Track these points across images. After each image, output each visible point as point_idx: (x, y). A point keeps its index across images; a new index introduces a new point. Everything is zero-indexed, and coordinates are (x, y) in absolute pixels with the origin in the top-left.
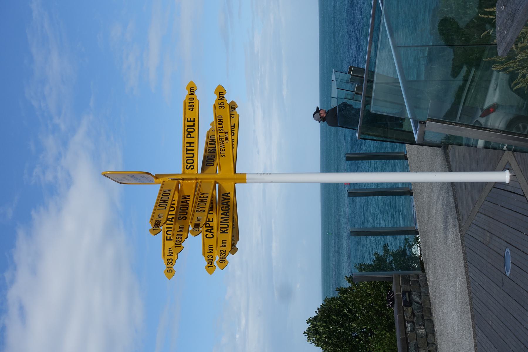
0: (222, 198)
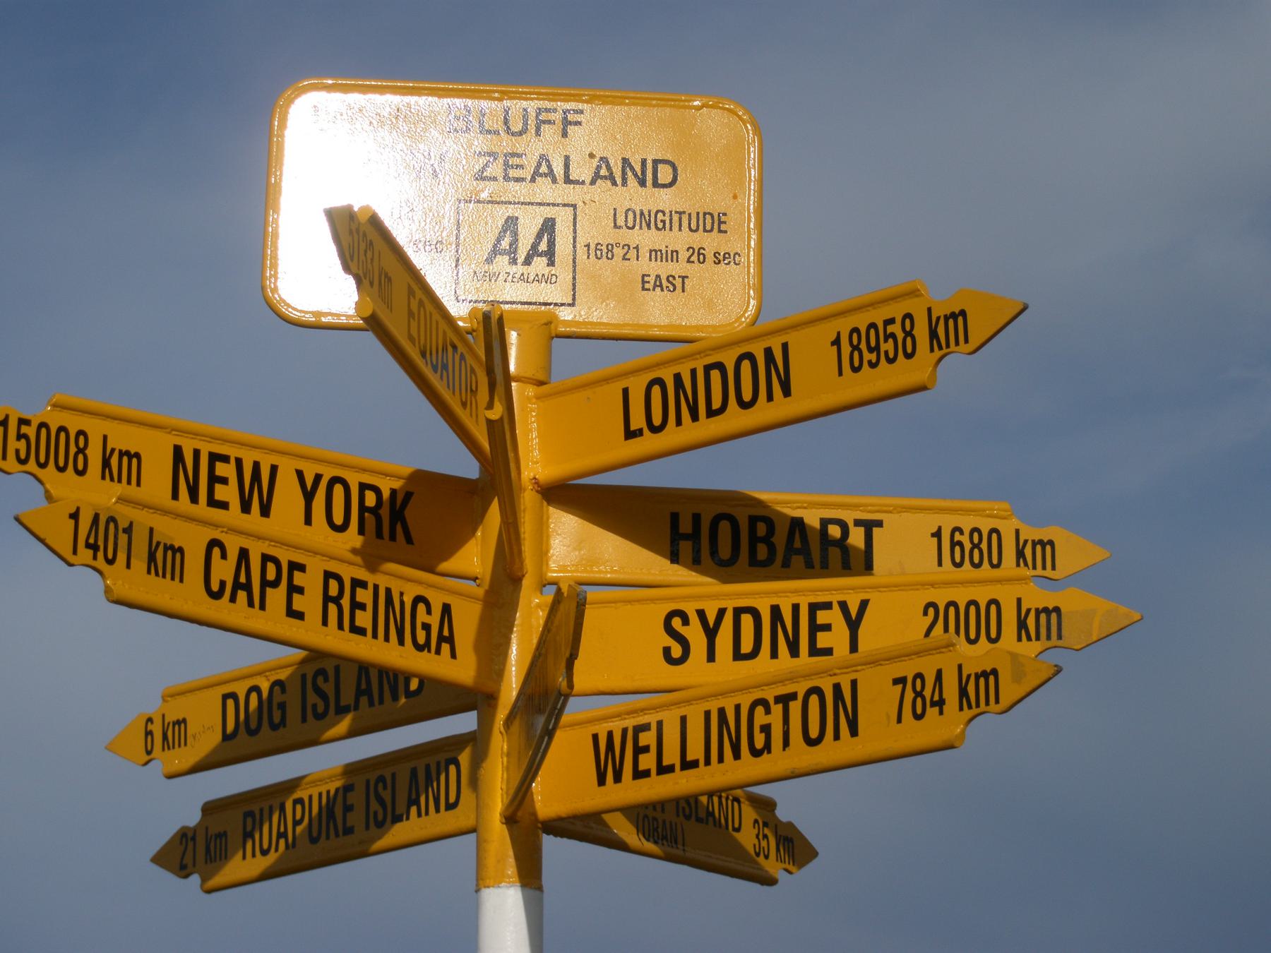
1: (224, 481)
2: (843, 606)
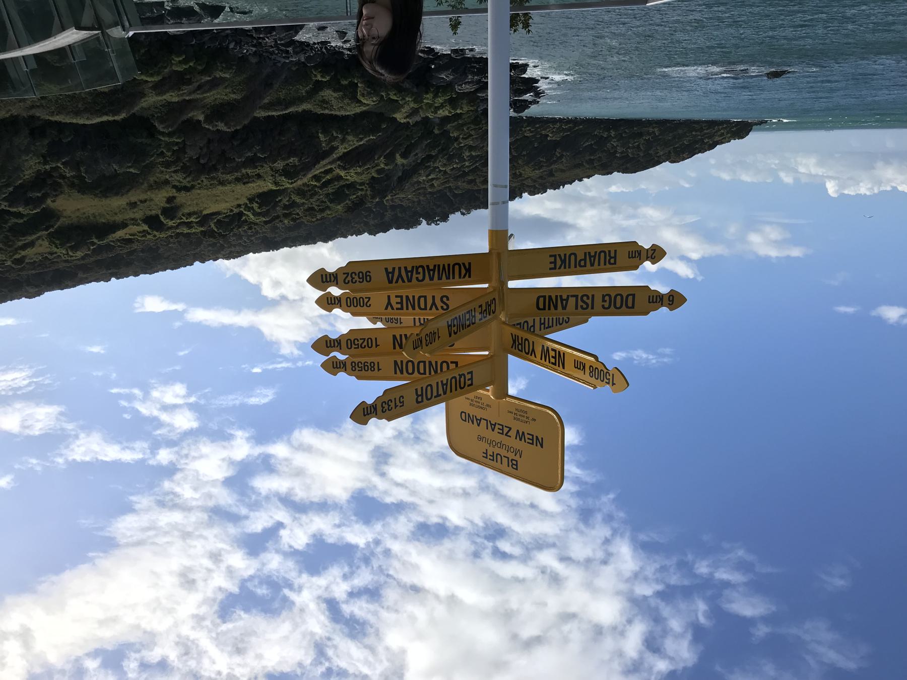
0: (397, 282)
1: (553, 357)
2: (393, 309)
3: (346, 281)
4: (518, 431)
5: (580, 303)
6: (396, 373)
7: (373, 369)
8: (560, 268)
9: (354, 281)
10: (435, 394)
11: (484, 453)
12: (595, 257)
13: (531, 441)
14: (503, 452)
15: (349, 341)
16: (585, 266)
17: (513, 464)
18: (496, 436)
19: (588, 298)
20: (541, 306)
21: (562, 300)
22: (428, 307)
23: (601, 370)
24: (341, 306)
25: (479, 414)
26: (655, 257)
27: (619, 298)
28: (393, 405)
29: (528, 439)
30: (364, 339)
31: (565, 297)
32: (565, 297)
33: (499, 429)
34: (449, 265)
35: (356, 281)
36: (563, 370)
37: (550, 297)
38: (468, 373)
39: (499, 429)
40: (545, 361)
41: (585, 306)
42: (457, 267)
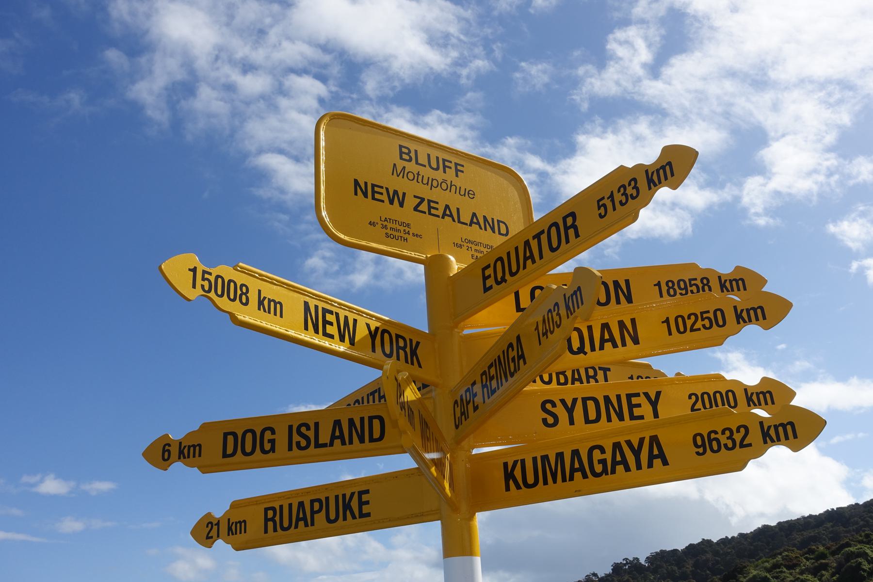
0: (642, 441)
1: (331, 324)
2: (647, 395)
3: (742, 430)
4: (401, 205)
5: (311, 434)
6: (627, 282)
7: (670, 284)
8: (353, 494)
9: (728, 433)
10: (544, 238)
11: (462, 172)
12: (298, 519)
13: (376, 189)
14: (427, 172)
15: (721, 323)
16: (312, 502)
17: (408, 154)
18: (442, 198)
19: (298, 443)
20: (376, 423)
21: (342, 437)
22: (579, 404)
23: (222, 296)
24: (746, 390)
25: (475, 233)
26: (207, 526)
27: (248, 449)
28: (618, 197)
29: (382, 194)
30: (692, 330)
31: (337, 442)
32: (337, 442)
33: (437, 209)
34: (545, 483)
35: (723, 433)
36: (307, 299)
37: (362, 440)
38: (491, 287)
39: (437, 209)
40: (346, 318)
41: (303, 429)
42: (531, 480)
